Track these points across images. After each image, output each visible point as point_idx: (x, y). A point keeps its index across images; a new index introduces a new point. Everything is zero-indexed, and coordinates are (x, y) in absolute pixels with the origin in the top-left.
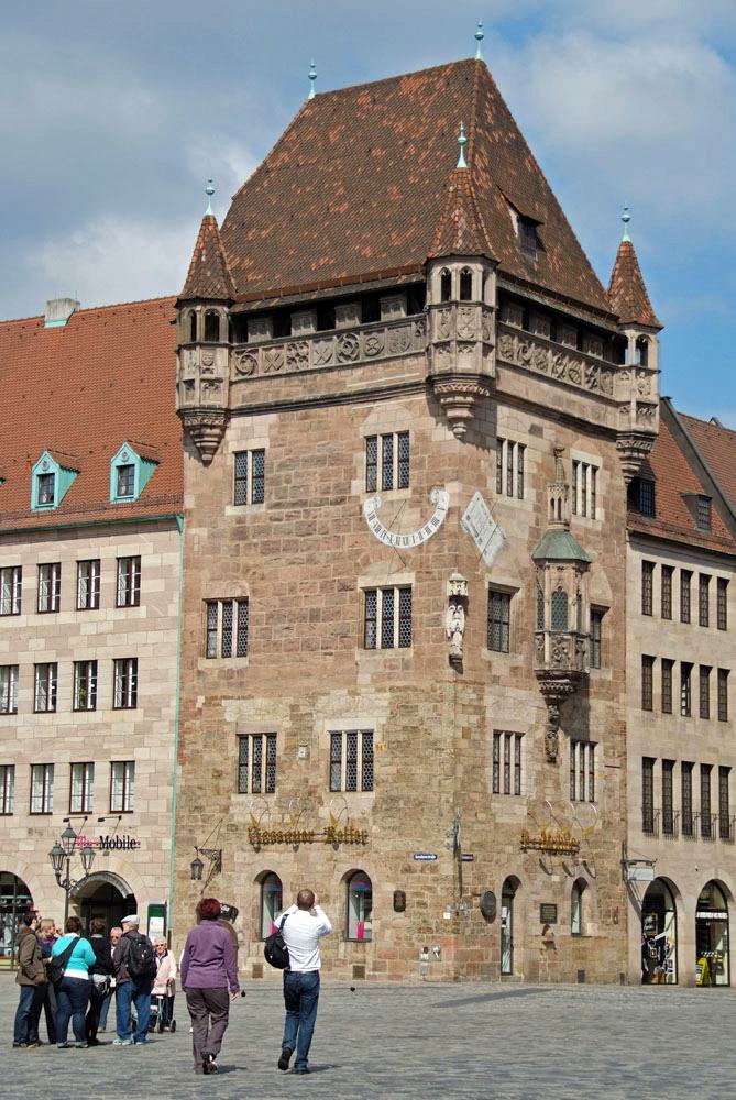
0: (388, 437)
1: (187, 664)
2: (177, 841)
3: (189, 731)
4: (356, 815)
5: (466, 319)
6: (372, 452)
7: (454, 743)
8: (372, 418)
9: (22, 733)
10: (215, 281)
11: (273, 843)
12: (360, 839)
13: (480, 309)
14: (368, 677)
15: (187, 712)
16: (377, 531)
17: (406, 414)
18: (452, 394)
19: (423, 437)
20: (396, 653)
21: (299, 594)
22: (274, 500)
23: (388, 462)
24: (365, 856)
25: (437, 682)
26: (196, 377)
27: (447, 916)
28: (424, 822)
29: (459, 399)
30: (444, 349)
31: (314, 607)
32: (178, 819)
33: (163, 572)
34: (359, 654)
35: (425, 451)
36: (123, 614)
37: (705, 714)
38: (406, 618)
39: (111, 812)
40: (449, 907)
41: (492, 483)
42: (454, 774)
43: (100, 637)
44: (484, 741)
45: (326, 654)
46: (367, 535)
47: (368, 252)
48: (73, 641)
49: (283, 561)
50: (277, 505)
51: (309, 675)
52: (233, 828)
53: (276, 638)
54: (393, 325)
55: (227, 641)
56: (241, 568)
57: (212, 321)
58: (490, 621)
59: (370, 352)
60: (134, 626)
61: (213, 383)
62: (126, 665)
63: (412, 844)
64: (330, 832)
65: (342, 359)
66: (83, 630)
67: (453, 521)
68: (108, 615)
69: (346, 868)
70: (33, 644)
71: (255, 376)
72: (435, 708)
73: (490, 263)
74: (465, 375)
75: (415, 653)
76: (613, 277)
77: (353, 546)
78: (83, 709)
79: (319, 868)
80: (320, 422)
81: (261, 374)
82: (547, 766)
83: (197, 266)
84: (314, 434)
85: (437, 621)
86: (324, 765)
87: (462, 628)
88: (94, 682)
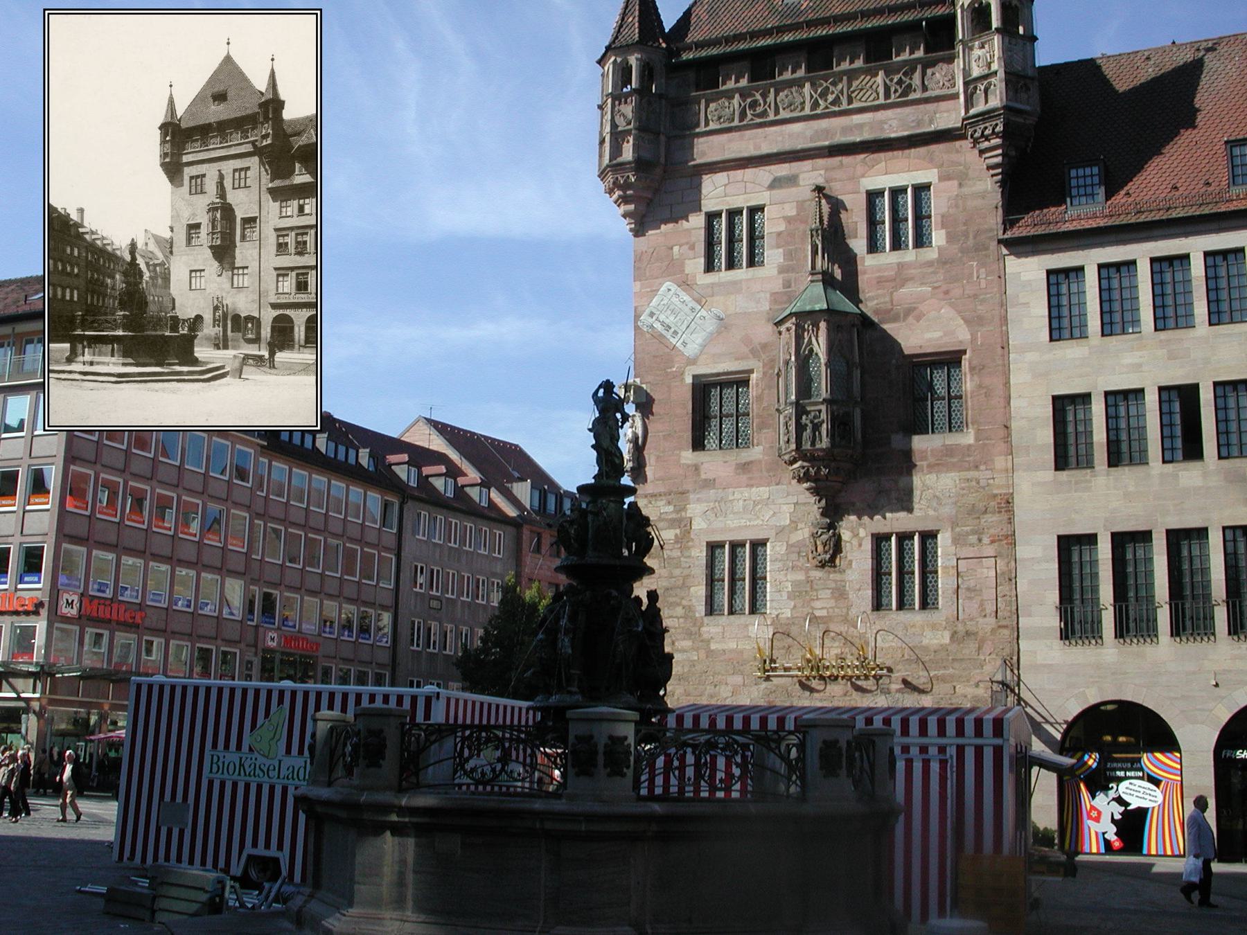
82: (818, 574)
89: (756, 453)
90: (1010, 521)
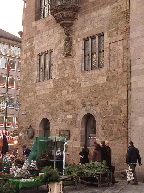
82: (66, 60)
90: (128, 22)
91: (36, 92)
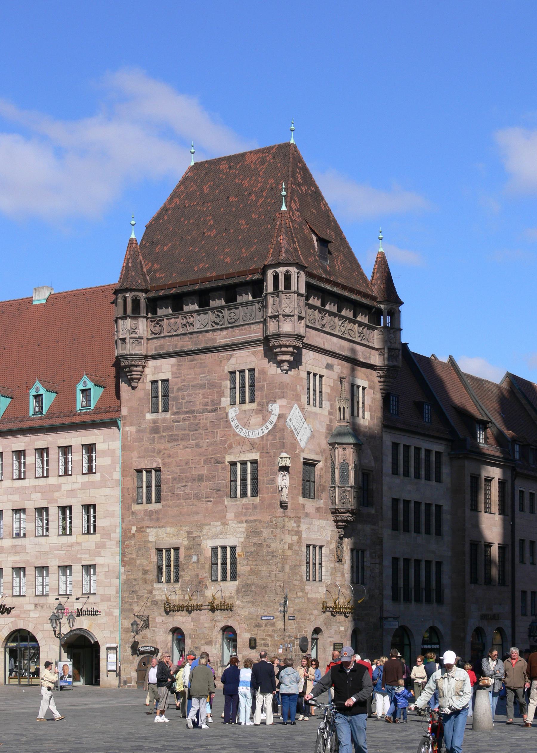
0: (242, 372)
1: (126, 507)
2: (122, 611)
3: (128, 546)
4: (227, 595)
5: (288, 301)
6: (233, 381)
7: (283, 552)
8: (233, 361)
9: (28, 548)
10: (137, 278)
11: (178, 611)
12: (228, 608)
13: (296, 295)
14: (233, 514)
15: (126, 536)
16: (237, 428)
17: (253, 359)
18: (280, 346)
19: (263, 372)
20: (249, 500)
21: (191, 466)
22: (175, 410)
23: (243, 387)
24: (233, 618)
25: (273, 517)
26: (127, 336)
27: (280, 651)
28: (267, 598)
29: (284, 349)
30: (275, 319)
31: (200, 473)
32: (123, 598)
33: (110, 453)
34: (227, 501)
35: (264, 380)
36: (87, 478)
37: (428, 532)
38: (255, 479)
39: (83, 594)
40: (281, 646)
41: (304, 399)
42: (283, 570)
43: (72, 492)
44: (301, 551)
45: (207, 501)
46: (231, 431)
47: (228, 260)
48: (57, 494)
49: (181, 446)
50: (177, 413)
51: (197, 514)
52: (155, 603)
53: (178, 492)
54: (245, 304)
55: (149, 493)
56: (156, 450)
57: (136, 302)
58: (303, 480)
59: (230, 321)
60: (93, 485)
61: (138, 340)
62: (89, 508)
63: (260, 611)
64: (211, 604)
65: (214, 324)
66: (63, 489)
67: (282, 422)
68: (78, 479)
69: (222, 625)
70: (34, 496)
71: (162, 335)
72: (272, 531)
73: (300, 267)
74: (288, 335)
75: (260, 500)
76: (374, 273)
77: (223, 437)
78: (64, 534)
79: (206, 625)
80: (201, 363)
81: (166, 334)
83: (126, 270)
84: (198, 370)
85: (273, 481)
86: (208, 566)
87: (287, 485)
88: (71, 518)
89: (321, 503)
91: (307, 593)
